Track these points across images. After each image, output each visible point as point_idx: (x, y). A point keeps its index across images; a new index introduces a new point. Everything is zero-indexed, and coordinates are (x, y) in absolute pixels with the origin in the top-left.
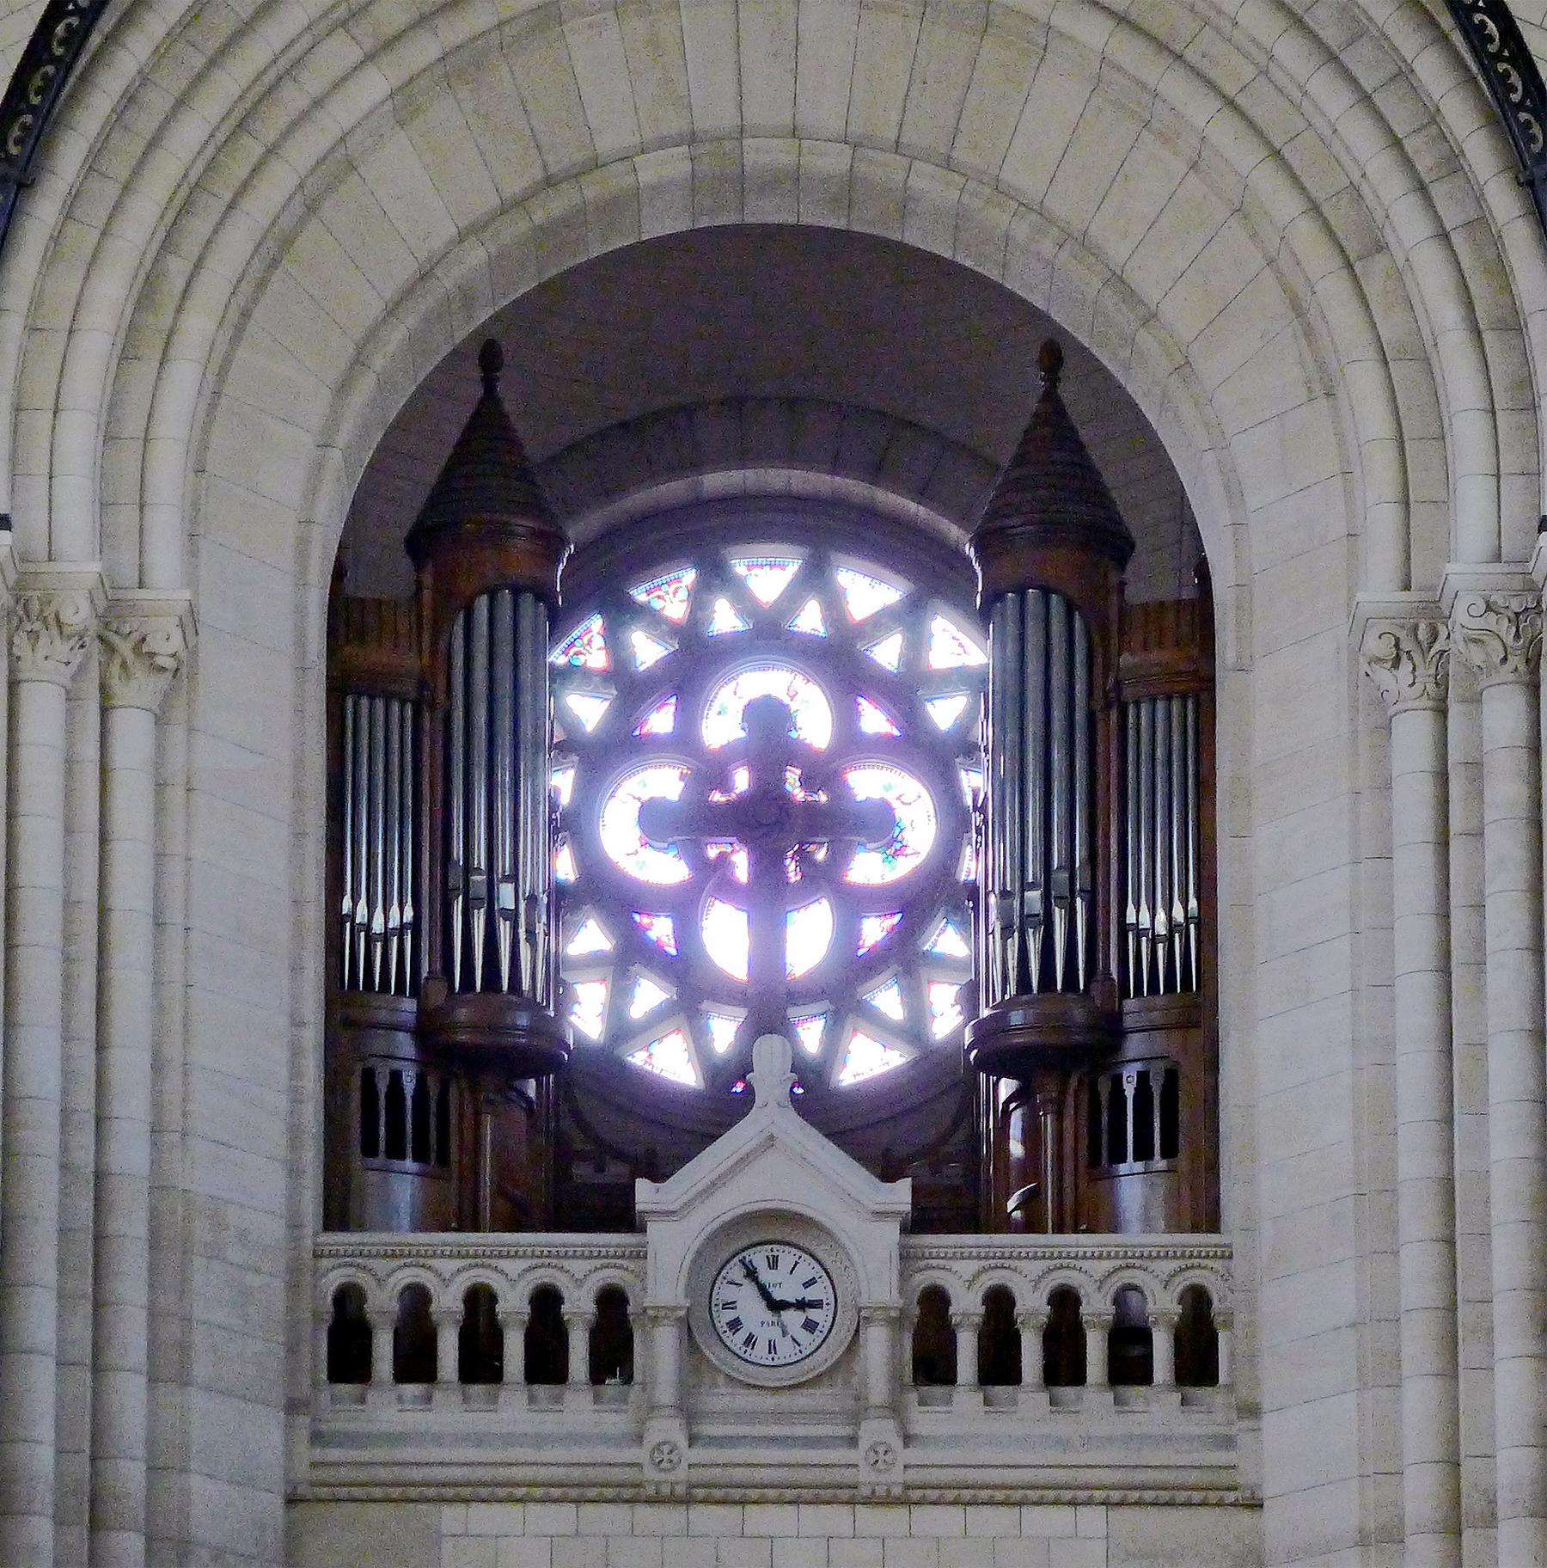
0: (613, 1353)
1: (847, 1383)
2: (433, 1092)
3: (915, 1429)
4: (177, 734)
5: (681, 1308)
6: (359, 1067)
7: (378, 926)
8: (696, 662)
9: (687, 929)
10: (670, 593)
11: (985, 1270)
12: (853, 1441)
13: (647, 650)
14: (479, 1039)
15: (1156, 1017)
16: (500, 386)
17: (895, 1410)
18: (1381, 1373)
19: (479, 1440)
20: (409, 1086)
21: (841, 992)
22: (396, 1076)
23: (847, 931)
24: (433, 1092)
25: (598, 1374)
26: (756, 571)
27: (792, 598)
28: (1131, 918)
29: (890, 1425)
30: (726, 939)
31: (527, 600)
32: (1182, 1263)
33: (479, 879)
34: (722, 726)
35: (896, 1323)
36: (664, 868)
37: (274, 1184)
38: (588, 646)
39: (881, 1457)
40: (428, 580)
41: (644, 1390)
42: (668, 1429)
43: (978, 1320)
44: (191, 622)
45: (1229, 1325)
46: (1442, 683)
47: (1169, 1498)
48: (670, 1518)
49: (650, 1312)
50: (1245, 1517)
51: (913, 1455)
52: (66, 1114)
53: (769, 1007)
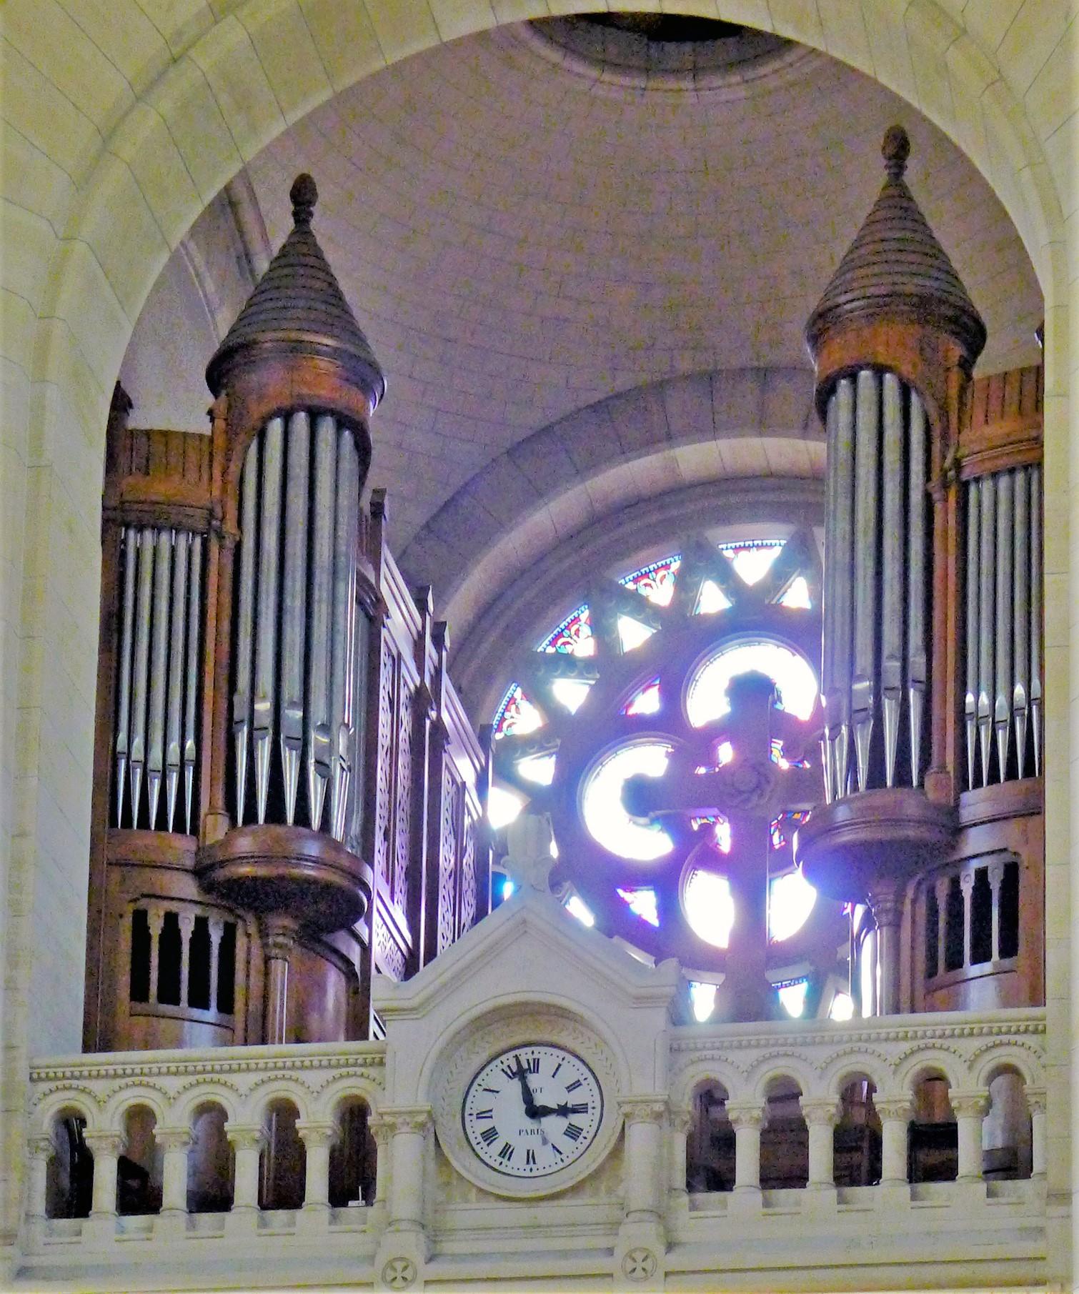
1: (610, 1191)
2: (216, 936)
5: (421, 1112)
6: (130, 908)
11: (765, 1059)
12: (610, 1252)
13: (633, 634)
14: (262, 871)
16: (315, 224)
17: (660, 1215)
20: (187, 929)
22: (171, 920)
24: (216, 936)
25: (339, 1197)
26: (743, 553)
27: (779, 577)
28: (970, 708)
30: (709, 907)
32: (990, 1040)
34: (707, 701)
36: (648, 844)
39: (639, 1265)
41: (384, 1207)
43: (757, 1113)
45: (1043, 1108)
49: (388, 1119)
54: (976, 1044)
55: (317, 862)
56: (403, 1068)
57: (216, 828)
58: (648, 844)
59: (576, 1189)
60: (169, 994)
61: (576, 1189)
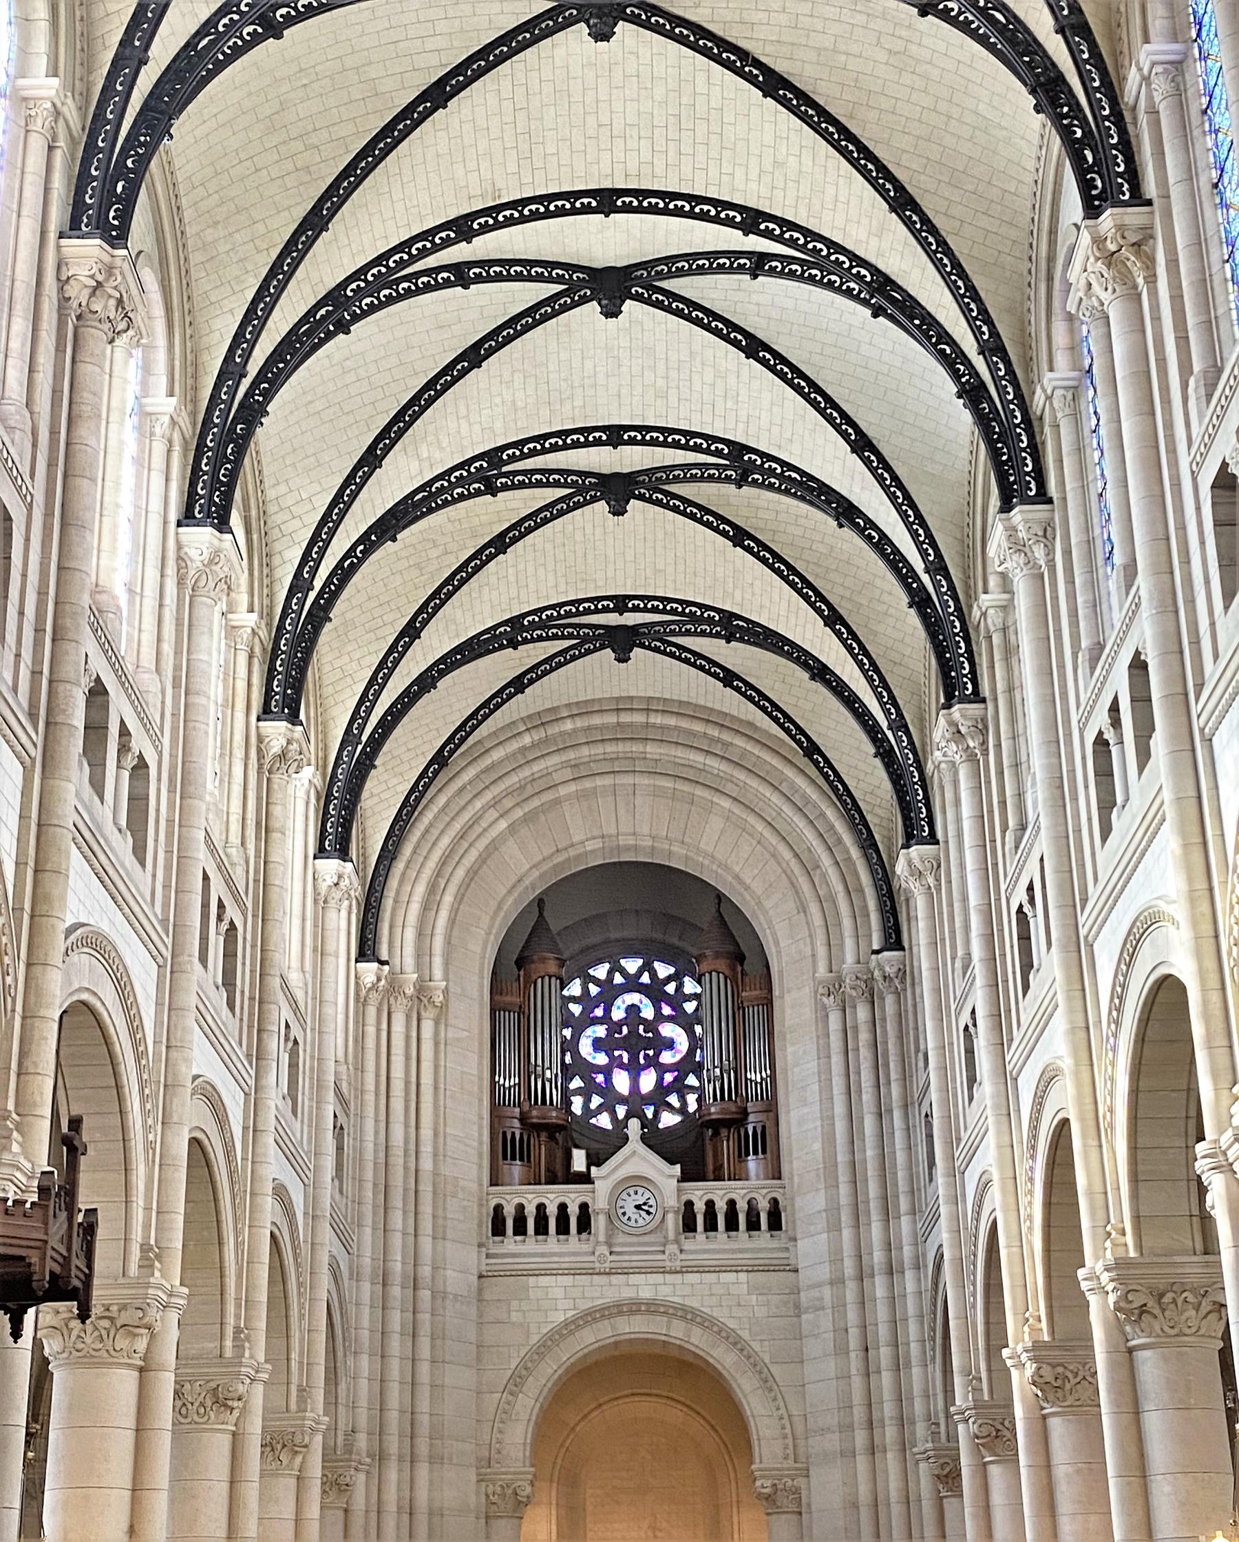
0: (585, 1224)
3: (685, 1248)
4: (442, 1027)
7: (507, 1085)
8: (610, 993)
9: (608, 1079)
10: (601, 972)
12: (664, 1252)
15: (759, 1108)
17: (677, 1241)
18: (834, 1227)
19: (542, 1255)
21: (658, 1097)
22: (513, 1134)
23: (660, 1080)
29: (676, 1246)
30: (621, 1081)
31: (553, 979)
33: (539, 1069)
34: (618, 1014)
35: (676, 1212)
36: (601, 1059)
37: (474, 1172)
38: (575, 989)
40: (522, 973)
42: (604, 1250)
44: (446, 991)
46: (844, 1001)
47: (767, 1269)
48: (604, 1279)
50: (790, 1274)
51: (683, 1256)
52: (406, 1151)
53: (635, 1101)
54: (765, 1191)
55: (557, 1117)
56: (600, 1192)
57: (526, 1107)
58: (601, 1059)
59: (650, 1232)
60: (513, 1158)
61: (650, 1232)
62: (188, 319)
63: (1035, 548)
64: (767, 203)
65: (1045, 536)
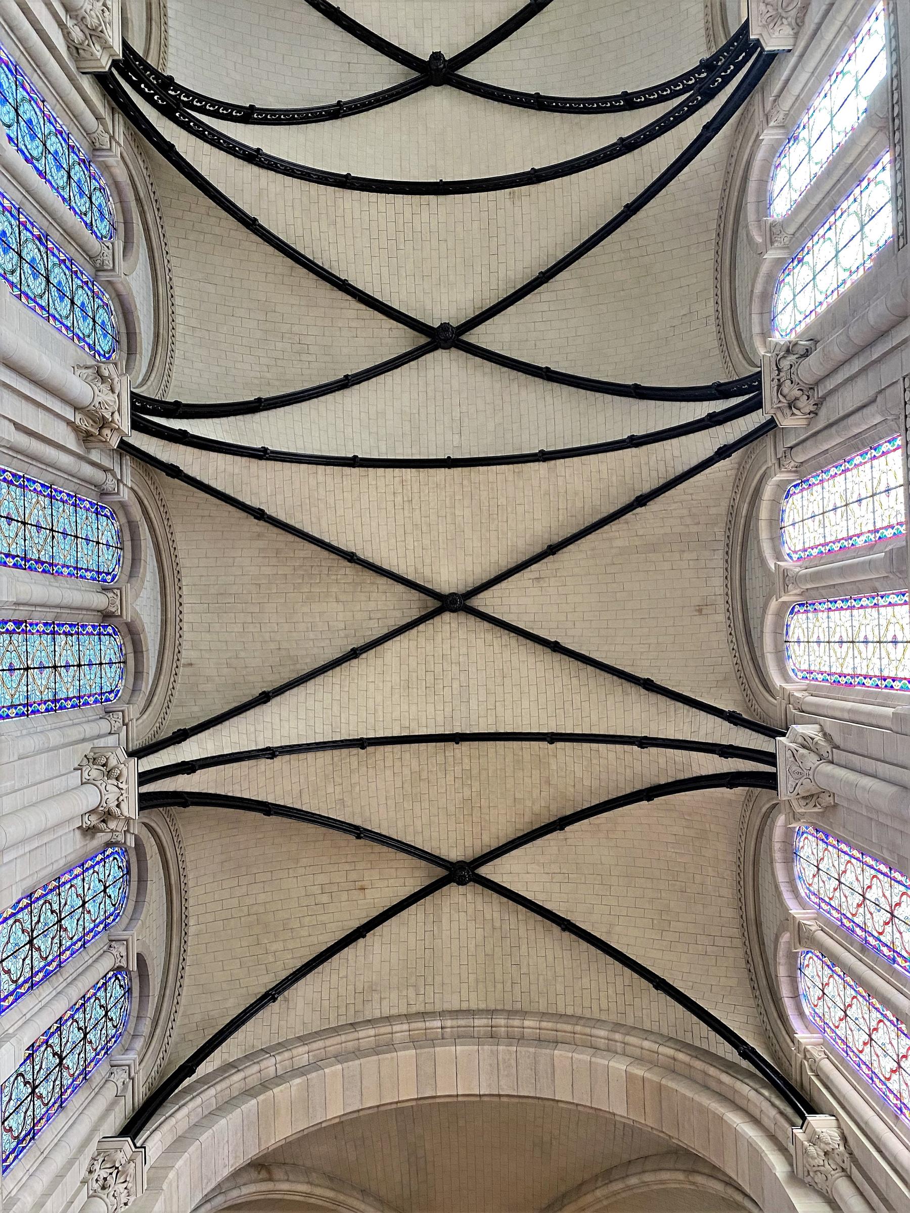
62: (733, 160)
63: (81, 34)
64: (344, 473)
65: (77, 49)
